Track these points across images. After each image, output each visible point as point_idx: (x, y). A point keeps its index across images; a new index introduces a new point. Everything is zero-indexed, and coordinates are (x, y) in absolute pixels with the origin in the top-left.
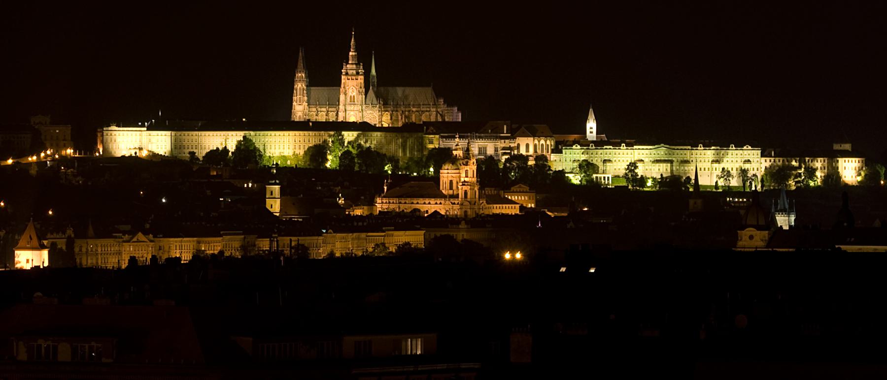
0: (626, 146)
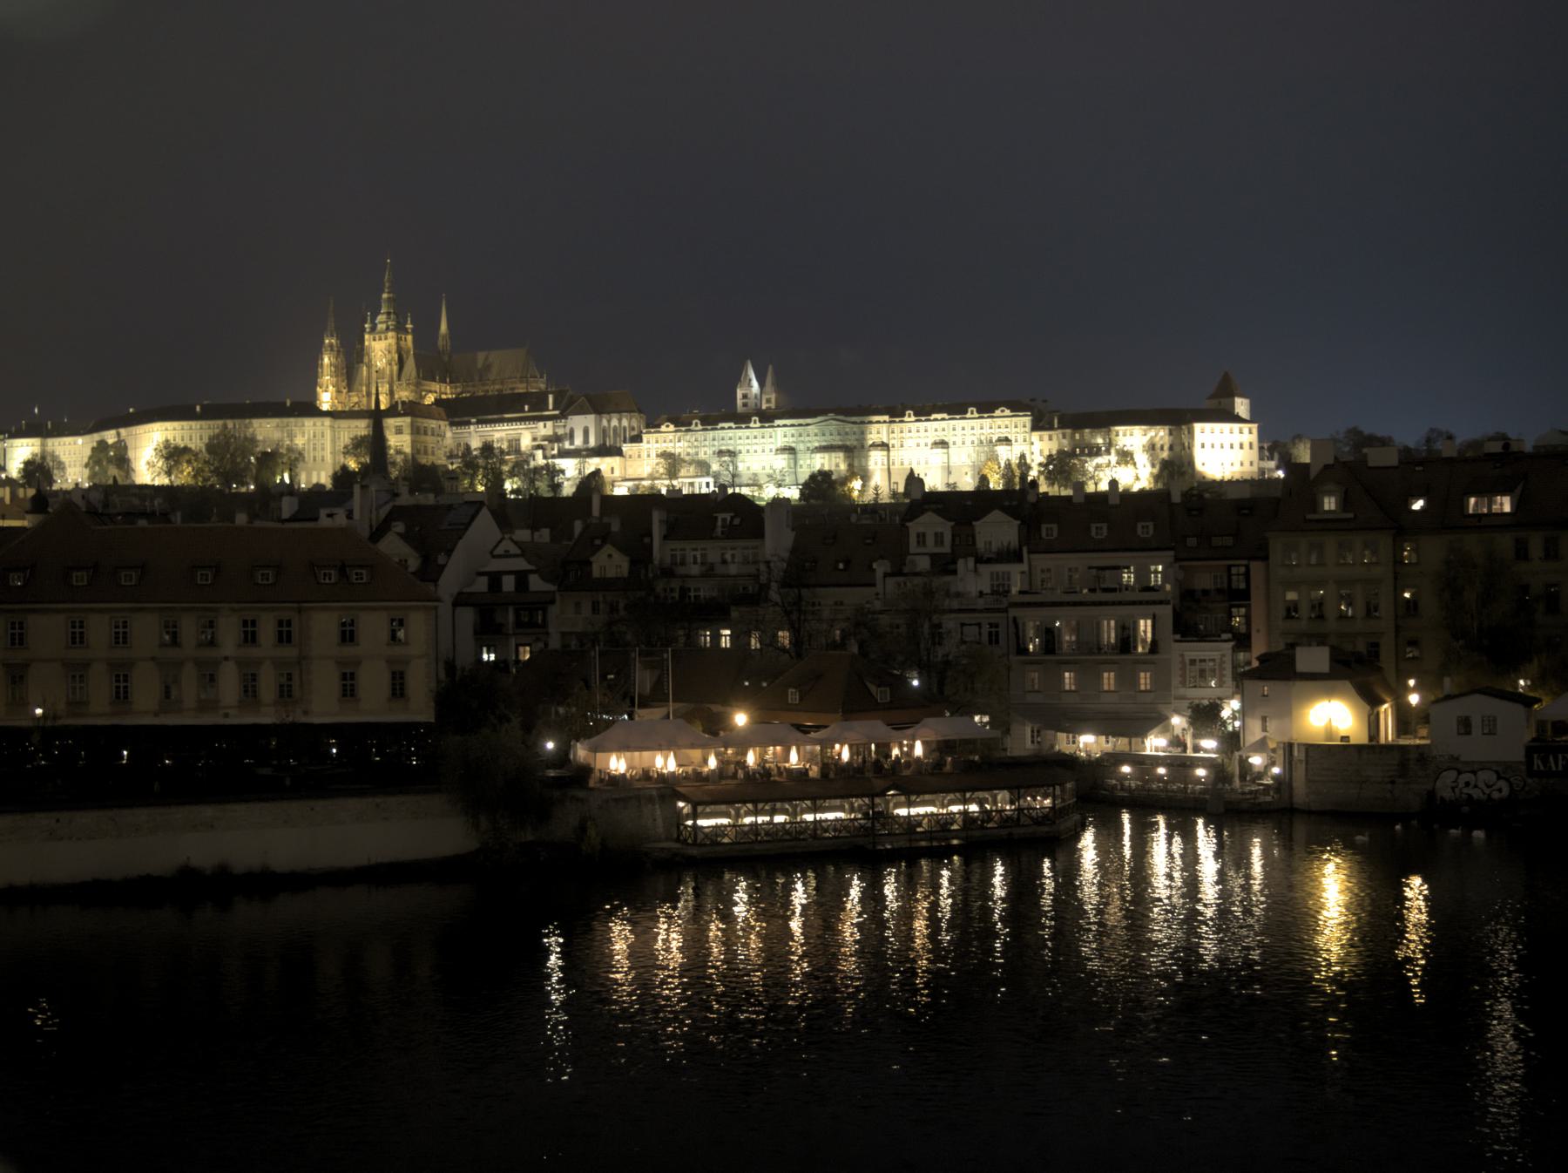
0: (760, 422)
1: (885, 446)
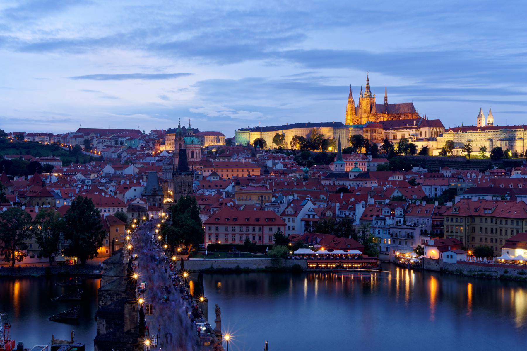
0: (481, 130)
1: (522, 139)
